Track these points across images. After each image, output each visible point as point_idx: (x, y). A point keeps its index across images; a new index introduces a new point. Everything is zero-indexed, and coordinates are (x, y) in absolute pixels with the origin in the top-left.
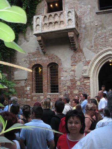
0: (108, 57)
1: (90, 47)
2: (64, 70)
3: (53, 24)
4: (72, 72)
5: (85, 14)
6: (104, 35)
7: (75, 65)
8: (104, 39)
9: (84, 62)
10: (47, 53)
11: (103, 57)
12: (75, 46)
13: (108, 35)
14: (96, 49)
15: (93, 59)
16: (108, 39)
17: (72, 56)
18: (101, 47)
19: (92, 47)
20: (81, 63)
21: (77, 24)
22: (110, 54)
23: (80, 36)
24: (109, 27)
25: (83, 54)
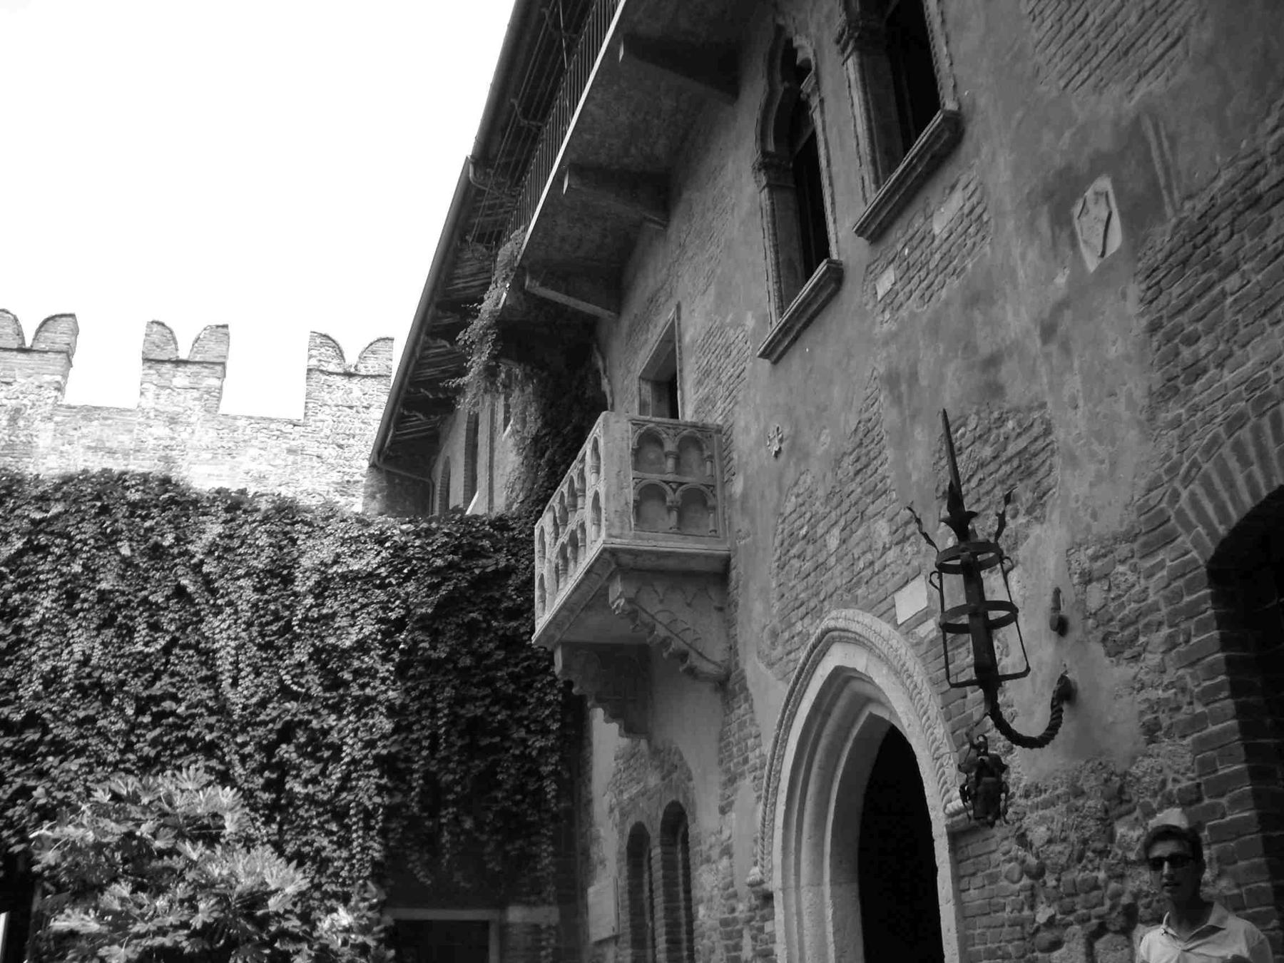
0: (842, 703)
2: (704, 847)
3: (569, 549)
4: (725, 862)
6: (808, 515)
7: (730, 804)
8: (810, 549)
9: (758, 773)
11: (816, 708)
13: (822, 510)
14: (789, 648)
17: (721, 739)
18: (807, 621)
19: (775, 635)
20: (749, 778)
22: (838, 671)
25: (751, 706)
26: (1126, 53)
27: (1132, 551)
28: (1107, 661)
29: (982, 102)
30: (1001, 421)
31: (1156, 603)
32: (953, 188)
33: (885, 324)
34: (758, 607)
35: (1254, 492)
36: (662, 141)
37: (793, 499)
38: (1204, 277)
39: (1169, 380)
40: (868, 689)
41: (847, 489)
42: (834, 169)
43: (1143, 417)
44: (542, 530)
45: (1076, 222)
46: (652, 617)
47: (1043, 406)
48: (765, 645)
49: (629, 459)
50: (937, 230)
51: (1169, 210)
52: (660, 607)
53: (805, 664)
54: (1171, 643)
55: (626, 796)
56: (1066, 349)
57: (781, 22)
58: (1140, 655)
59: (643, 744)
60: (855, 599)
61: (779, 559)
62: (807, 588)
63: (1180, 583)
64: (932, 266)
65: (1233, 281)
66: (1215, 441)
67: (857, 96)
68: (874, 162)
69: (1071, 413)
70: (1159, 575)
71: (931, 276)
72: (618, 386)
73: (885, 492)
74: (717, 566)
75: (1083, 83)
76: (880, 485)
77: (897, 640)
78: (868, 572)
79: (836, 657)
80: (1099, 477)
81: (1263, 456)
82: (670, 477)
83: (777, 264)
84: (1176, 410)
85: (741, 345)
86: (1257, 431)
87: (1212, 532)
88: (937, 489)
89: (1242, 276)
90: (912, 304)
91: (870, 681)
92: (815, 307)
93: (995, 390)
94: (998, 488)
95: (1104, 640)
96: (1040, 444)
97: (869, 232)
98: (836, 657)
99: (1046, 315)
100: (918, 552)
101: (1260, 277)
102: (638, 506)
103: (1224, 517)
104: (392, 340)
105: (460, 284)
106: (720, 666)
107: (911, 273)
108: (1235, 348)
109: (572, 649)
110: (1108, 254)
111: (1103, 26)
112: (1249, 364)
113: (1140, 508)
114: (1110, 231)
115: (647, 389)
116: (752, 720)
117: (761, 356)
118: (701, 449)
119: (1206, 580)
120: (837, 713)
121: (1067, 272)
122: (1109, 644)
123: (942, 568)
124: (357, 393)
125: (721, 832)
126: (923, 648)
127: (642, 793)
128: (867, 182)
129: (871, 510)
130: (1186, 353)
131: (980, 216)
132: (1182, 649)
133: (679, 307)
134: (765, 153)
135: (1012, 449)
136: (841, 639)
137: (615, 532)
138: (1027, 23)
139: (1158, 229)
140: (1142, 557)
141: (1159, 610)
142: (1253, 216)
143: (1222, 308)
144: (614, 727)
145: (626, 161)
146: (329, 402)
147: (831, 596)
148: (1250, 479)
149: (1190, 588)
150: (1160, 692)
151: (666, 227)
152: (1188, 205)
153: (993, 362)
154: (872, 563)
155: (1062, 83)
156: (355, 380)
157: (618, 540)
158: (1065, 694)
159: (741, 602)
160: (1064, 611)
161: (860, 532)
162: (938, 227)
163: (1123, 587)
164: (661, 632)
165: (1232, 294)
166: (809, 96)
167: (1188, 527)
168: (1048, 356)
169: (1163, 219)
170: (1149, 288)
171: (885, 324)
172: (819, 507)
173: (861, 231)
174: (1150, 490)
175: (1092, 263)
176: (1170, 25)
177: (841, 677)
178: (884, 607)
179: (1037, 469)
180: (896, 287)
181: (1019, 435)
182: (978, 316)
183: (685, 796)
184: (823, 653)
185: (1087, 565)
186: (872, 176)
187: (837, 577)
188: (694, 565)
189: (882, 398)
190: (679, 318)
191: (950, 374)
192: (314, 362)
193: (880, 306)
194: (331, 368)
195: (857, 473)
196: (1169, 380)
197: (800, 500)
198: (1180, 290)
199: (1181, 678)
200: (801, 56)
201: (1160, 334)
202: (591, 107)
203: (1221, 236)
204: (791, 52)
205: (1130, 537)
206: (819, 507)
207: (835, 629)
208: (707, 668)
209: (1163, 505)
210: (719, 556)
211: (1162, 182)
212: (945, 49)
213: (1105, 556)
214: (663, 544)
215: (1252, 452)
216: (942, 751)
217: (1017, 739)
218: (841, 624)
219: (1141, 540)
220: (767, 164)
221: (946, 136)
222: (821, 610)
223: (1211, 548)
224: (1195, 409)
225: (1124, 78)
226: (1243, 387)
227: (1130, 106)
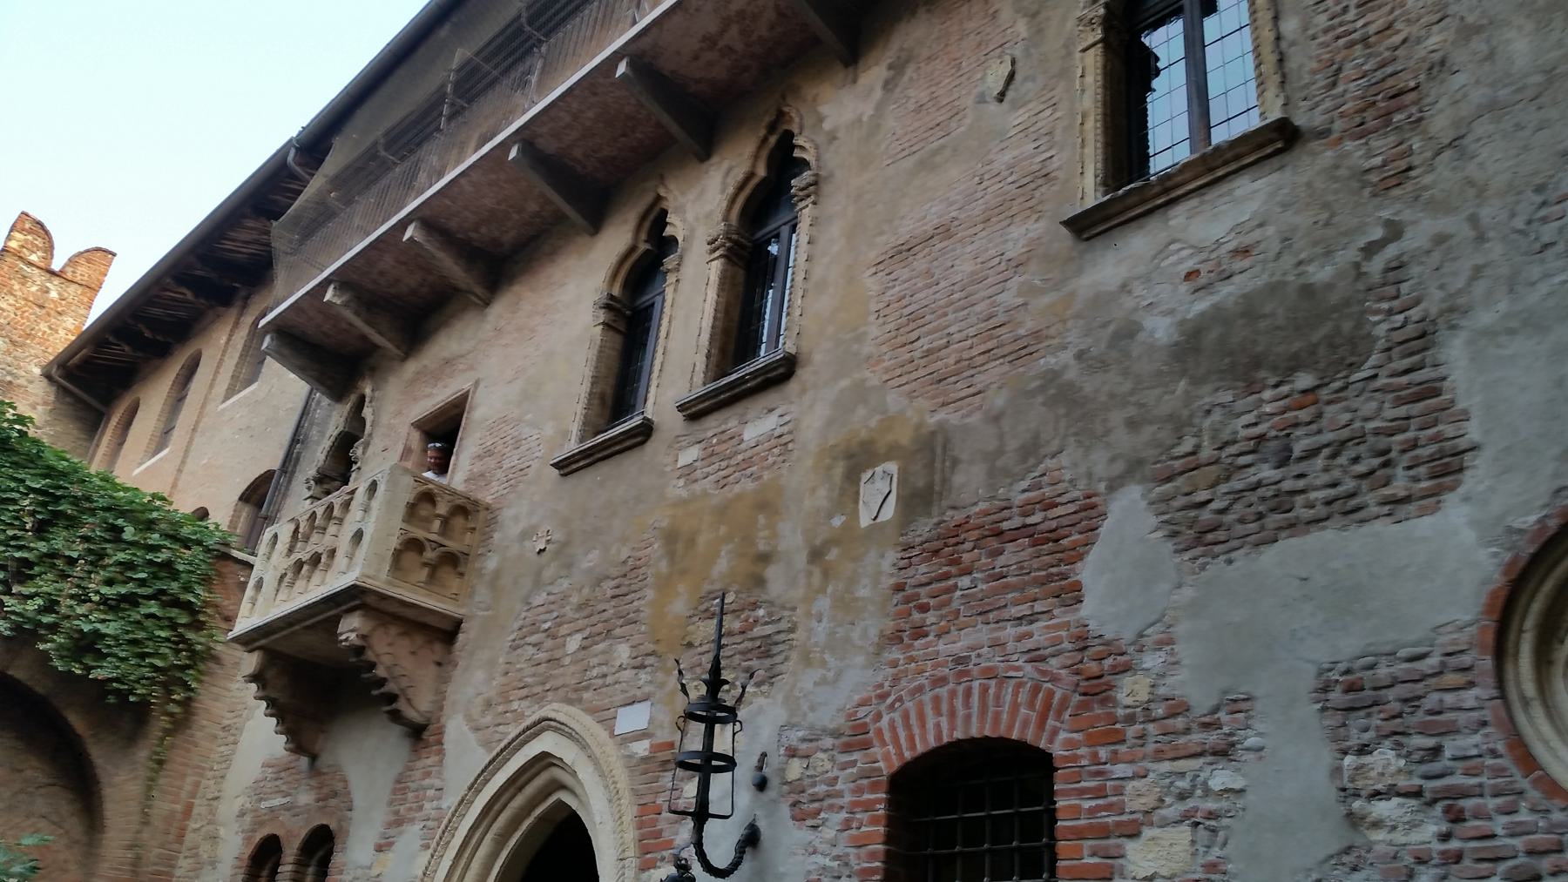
1: (480, 709)
3: (306, 568)
5: (521, 486)
6: (555, 614)
7: (391, 844)
8: (549, 643)
9: (430, 823)
10: (325, 760)
12: (394, 706)
13: (571, 615)
15: (460, 798)
16: (564, 645)
17: (398, 781)
18: (525, 703)
19: (488, 704)
20: (417, 827)
21: (430, 555)
23: (461, 637)
24: (591, 556)
25: (441, 761)
26: (940, 381)
27: (834, 745)
28: (791, 822)
29: (818, 358)
30: (755, 606)
31: (842, 791)
32: (771, 411)
33: (677, 489)
34: (479, 675)
35: (939, 735)
36: (513, 233)
37: (544, 594)
38: (945, 569)
39: (898, 631)
40: (566, 778)
41: (601, 607)
42: (671, 345)
43: (871, 649)
44: (276, 536)
45: (862, 484)
46: (378, 656)
47: (794, 609)
48: (476, 711)
49: (401, 510)
50: (746, 436)
51: (935, 510)
52: (387, 649)
53: (513, 740)
54: (847, 825)
55: (264, 805)
56: (826, 575)
57: (662, 192)
58: (818, 827)
59: (304, 761)
60: (580, 700)
61: (514, 640)
62: (534, 675)
63: (865, 782)
64: (733, 462)
65: (965, 581)
66: (920, 689)
67: (712, 295)
68: (708, 356)
69: (814, 624)
70: (850, 770)
71: (731, 470)
72: (385, 419)
73: (636, 622)
74: (446, 626)
75: (899, 386)
76: (632, 615)
77: (610, 746)
78: (600, 682)
79: (546, 743)
80: (822, 682)
81: (952, 714)
82: (434, 537)
83: (591, 394)
84: (895, 654)
85: (532, 444)
86: (953, 694)
87: (900, 754)
88: (683, 638)
89: (972, 582)
90: (707, 484)
91: (574, 774)
92: (618, 448)
93: (760, 582)
94: (737, 656)
95: (794, 805)
96: (782, 637)
97: (689, 412)
98: (546, 743)
99: (818, 542)
100: (651, 682)
101: (984, 587)
102: (398, 555)
103: (913, 746)
104: (114, 255)
105: (228, 245)
106: (422, 715)
107: (713, 459)
108: (952, 628)
109: (272, 656)
110: (878, 520)
111: (929, 353)
112: (959, 644)
113: (850, 715)
114: (884, 505)
115: (416, 436)
116: (440, 773)
117: (556, 465)
118: (467, 519)
119: (885, 787)
120: (530, 790)
121: (844, 518)
122: (796, 810)
123: (690, 716)
124: (54, 294)
125: (370, 868)
126: (634, 762)
127: (287, 808)
128: (697, 369)
129: (618, 631)
130: (916, 616)
131: (786, 444)
132: (854, 832)
133: (477, 384)
134: (612, 297)
135: (758, 631)
136: (556, 730)
137: (371, 573)
138: (872, 318)
139: (923, 520)
140: (839, 752)
141: (843, 797)
142: (994, 543)
143: (951, 597)
144: (283, 738)
145: (474, 235)
146: (19, 293)
147: (557, 689)
148: (938, 725)
149: (874, 788)
150: (827, 860)
151: (487, 303)
152: (950, 513)
153: (765, 558)
154: (605, 676)
155: (886, 377)
156: (56, 281)
157: (370, 581)
158: (751, 839)
159: (461, 663)
160: (766, 771)
161: (601, 646)
162: (751, 433)
163: (819, 770)
164: (380, 672)
165: (961, 590)
166: (669, 271)
167: (884, 744)
168: (810, 574)
169: (929, 515)
170: (902, 559)
171: (677, 489)
172: (568, 611)
173: (681, 408)
174: (859, 705)
175: (865, 521)
176: (978, 378)
177: (544, 760)
178: (607, 714)
179: (775, 655)
180: (696, 464)
181: (767, 623)
182: (762, 519)
183: (340, 821)
184: (536, 735)
185: (794, 743)
186: (704, 366)
187: (568, 675)
188: (430, 620)
189: (656, 546)
190: (474, 393)
191: (723, 553)
192: (13, 244)
193: (678, 473)
194: (34, 258)
195: (614, 597)
196: (898, 631)
197: (552, 598)
198: (925, 570)
199: (848, 855)
200: (668, 231)
201: (901, 594)
202: (463, 181)
203: (968, 545)
204: (661, 220)
205: (836, 734)
206: (568, 611)
207: (555, 720)
208: (411, 714)
209: (868, 720)
210: (455, 618)
211: (937, 488)
212: (800, 301)
213: (811, 741)
214: (407, 594)
215: (945, 707)
216: (627, 854)
217: (708, 867)
218: (561, 717)
219: (845, 739)
220: (610, 305)
221: (781, 370)
222: (543, 698)
223: (897, 764)
224: (912, 659)
225: (934, 397)
226: (951, 658)
227: (932, 420)
